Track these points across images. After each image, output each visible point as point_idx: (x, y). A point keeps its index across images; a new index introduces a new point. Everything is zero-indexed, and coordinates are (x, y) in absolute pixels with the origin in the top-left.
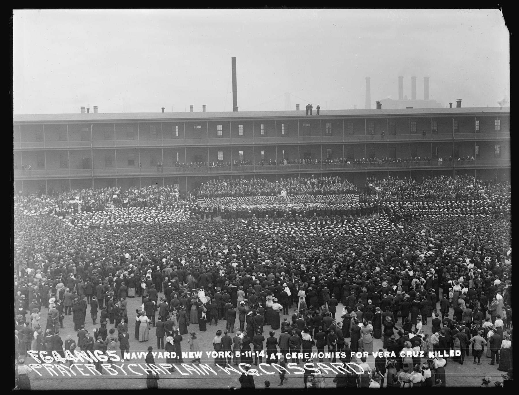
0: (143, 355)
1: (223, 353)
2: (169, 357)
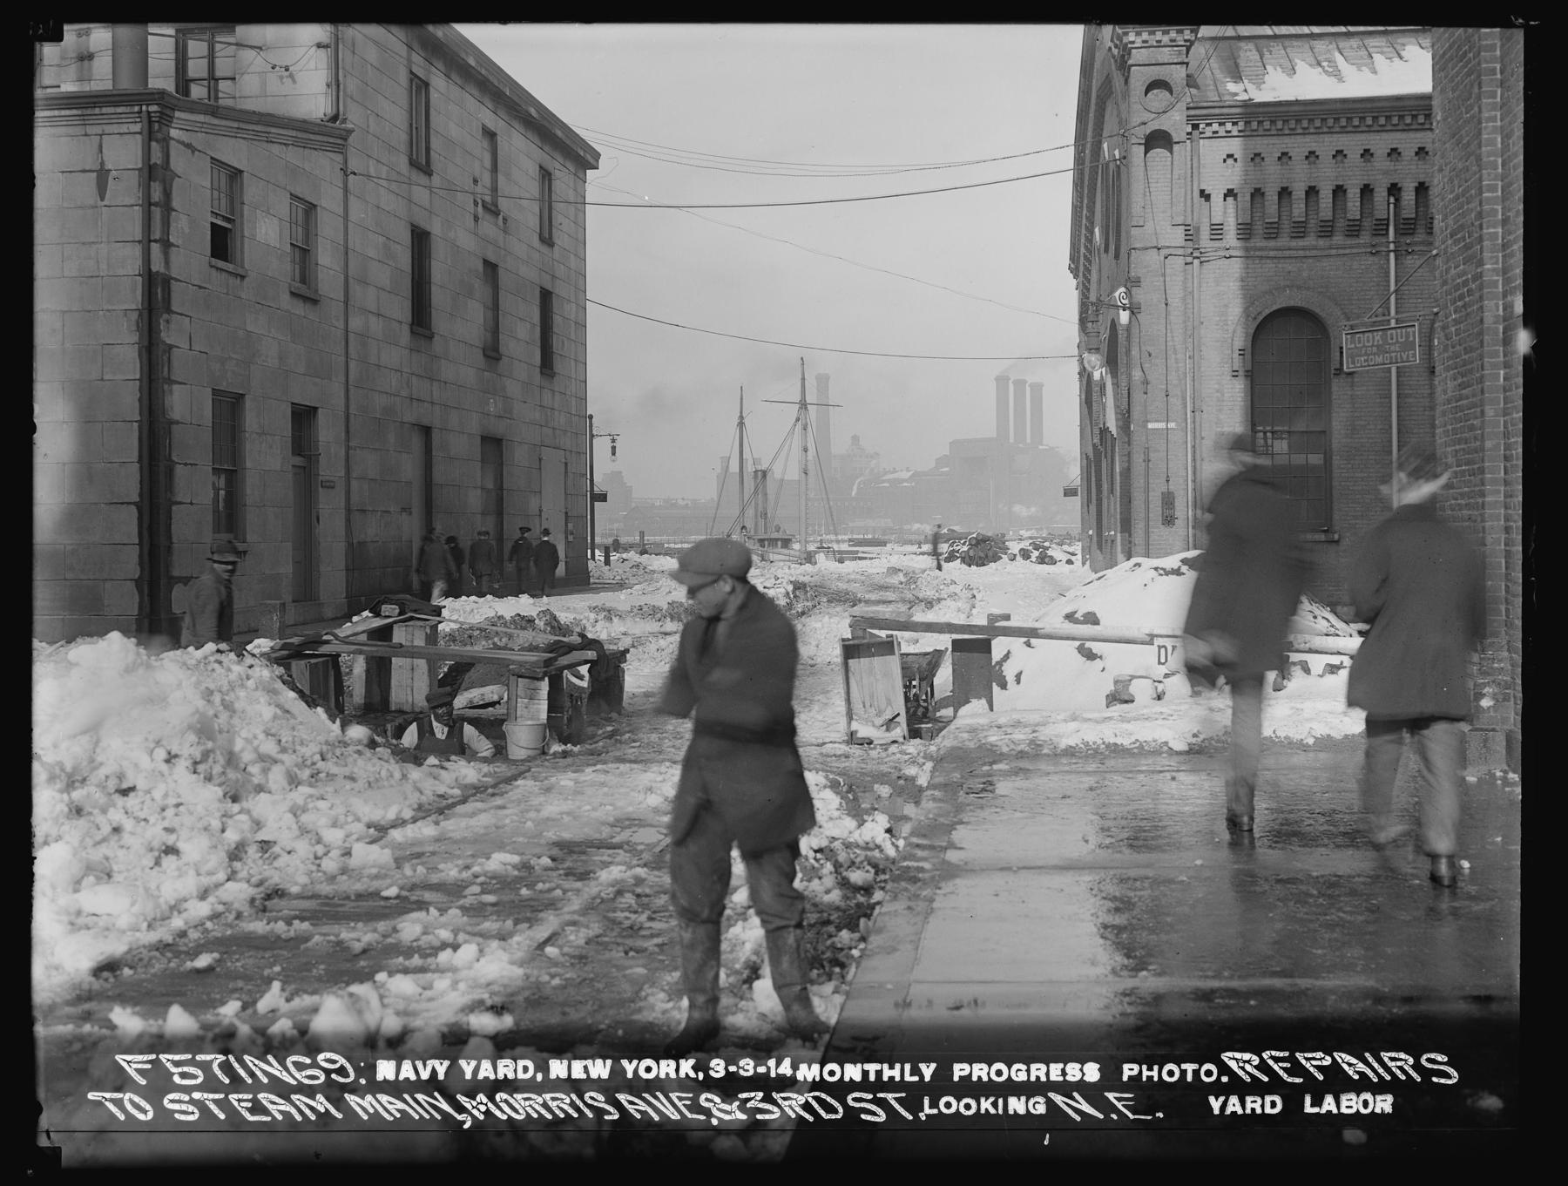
0: (434, 1072)
1: (673, 1063)
2: (511, 1076)
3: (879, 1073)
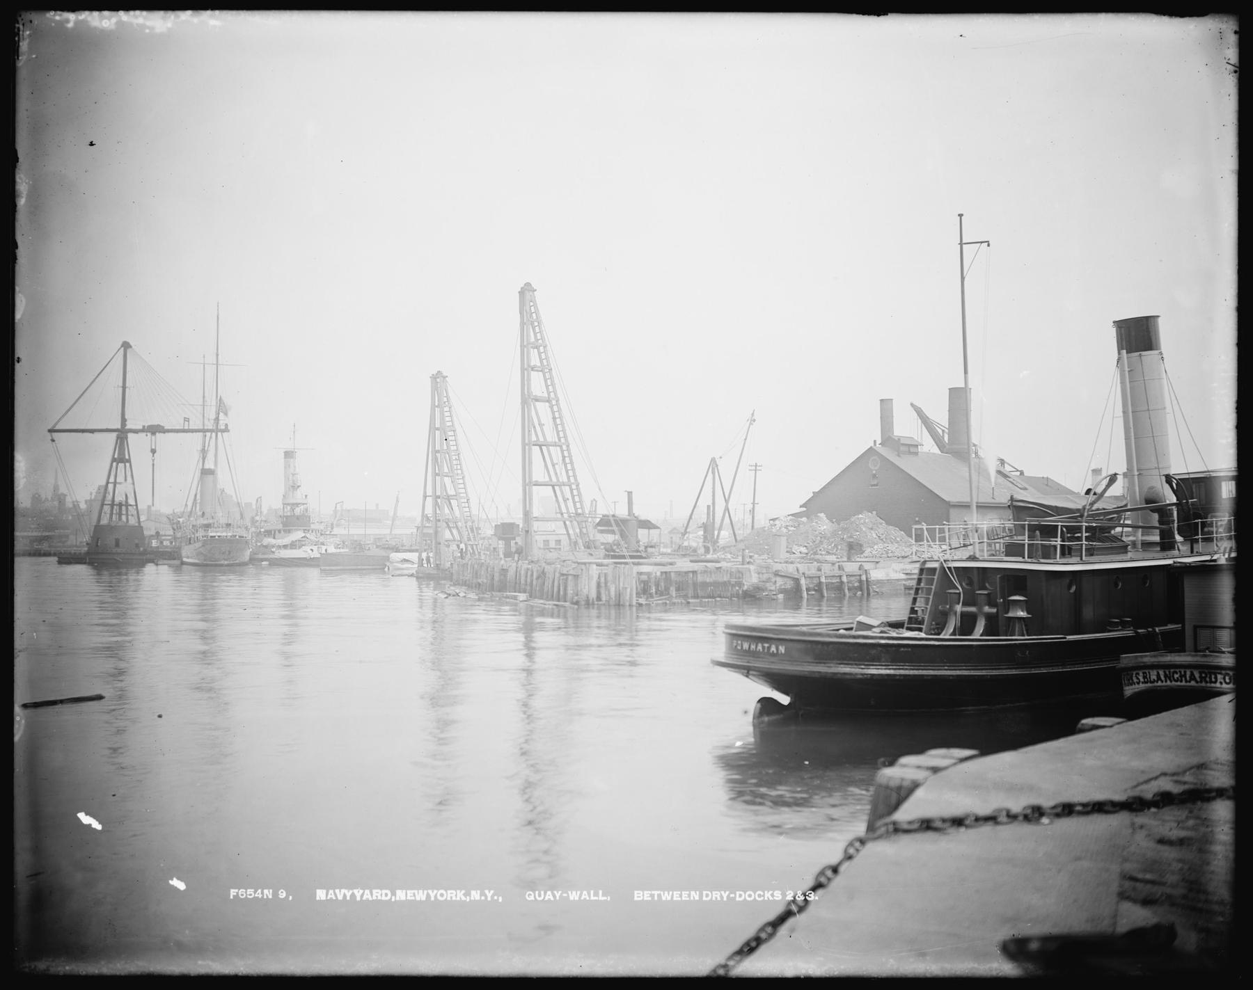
0: (345, 896)
1: (454, 892)
3: (659, 896)
